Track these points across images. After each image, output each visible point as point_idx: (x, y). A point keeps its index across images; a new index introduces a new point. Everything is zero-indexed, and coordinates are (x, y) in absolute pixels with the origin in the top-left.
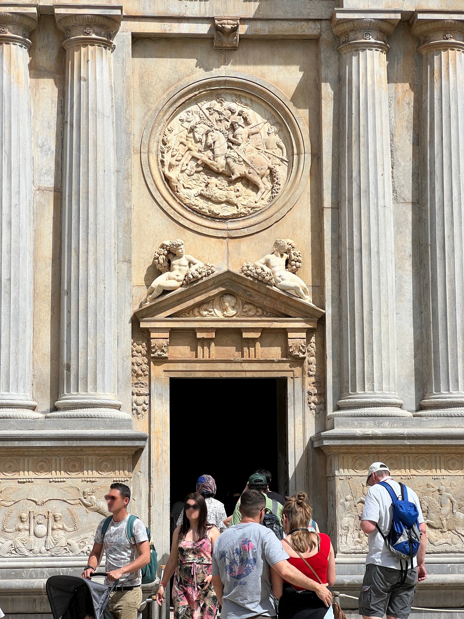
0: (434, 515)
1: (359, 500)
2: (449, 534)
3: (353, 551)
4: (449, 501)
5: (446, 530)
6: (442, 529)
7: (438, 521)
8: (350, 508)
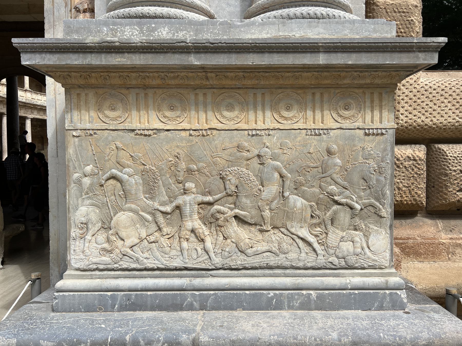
0: (248, 202)
1: (107, 175)
2: (275, 236)
3: (95, 267)
4: (276, 175)
5: (270, 228)
6: (261, 226)
7: (254, 212)
8: (91, 188)
